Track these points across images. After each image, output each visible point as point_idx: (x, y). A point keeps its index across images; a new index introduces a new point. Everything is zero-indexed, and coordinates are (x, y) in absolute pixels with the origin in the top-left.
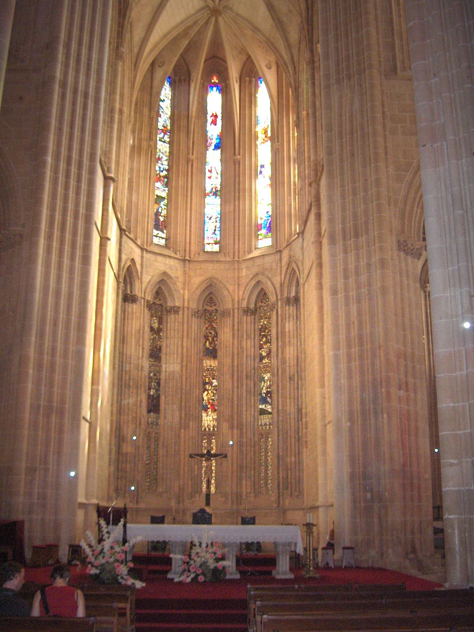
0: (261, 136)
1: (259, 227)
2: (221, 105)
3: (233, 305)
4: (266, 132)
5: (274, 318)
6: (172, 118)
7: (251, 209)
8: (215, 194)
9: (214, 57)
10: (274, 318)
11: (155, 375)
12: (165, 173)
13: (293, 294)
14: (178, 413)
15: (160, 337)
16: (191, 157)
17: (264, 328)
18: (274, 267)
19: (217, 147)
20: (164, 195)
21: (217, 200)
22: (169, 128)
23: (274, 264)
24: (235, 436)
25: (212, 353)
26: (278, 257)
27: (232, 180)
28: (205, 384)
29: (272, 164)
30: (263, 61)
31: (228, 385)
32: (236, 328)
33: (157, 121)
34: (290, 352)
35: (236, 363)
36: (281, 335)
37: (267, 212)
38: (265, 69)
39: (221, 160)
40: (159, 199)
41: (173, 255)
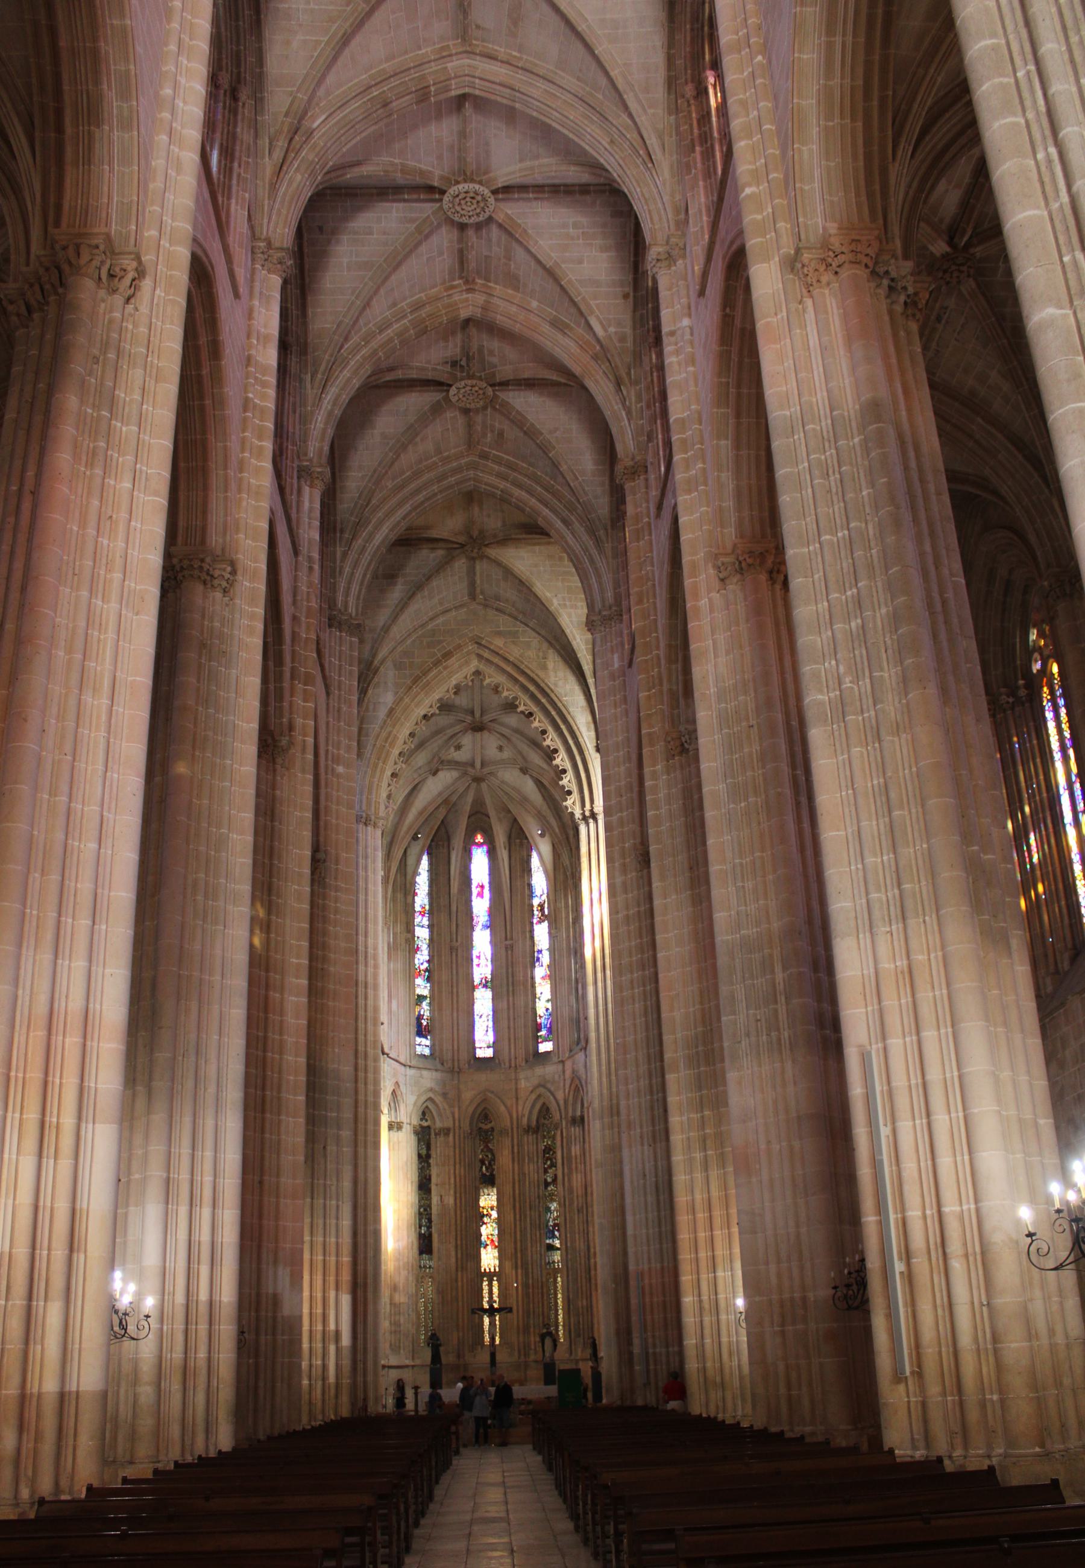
0: (536, 913)
1: (539, 1028)
2: (487, 871)
3: (512, 1123)
4: (542, 910)
5: (558, 1138)
6: (431, 894)
7: (526, 1006)
8: (485, 986)
9: (477, 813)
10: (558, 1138)
11: (425, 1210)
12: (426, 965)
13: (579, 1113)
14: (453, 1253)
15: (429, 1165)
16: (454, 944)
17: (548, 1149)
18: (556, 1077)
19: (485, 927)
20: (426, 992)
21: (488, 994)
22: (427, 907)
23: (556, 1077)
24: (520, 1278)
25: (489, 1181)
26: (560, 1067)
27: (504, 970)
28: (483, 1216)
29: (549, 950)
30: (534, 831)
31: (510, 1217)
32: (516, 1151)
33: (414, 902)
34: (577, 1180)
35: (517, 1192)
36: (568, 1159)
37: (547, 1010)
38: (538, 839)
39: (491, 942)
40: (421, 998)
41: (439, 1066)
